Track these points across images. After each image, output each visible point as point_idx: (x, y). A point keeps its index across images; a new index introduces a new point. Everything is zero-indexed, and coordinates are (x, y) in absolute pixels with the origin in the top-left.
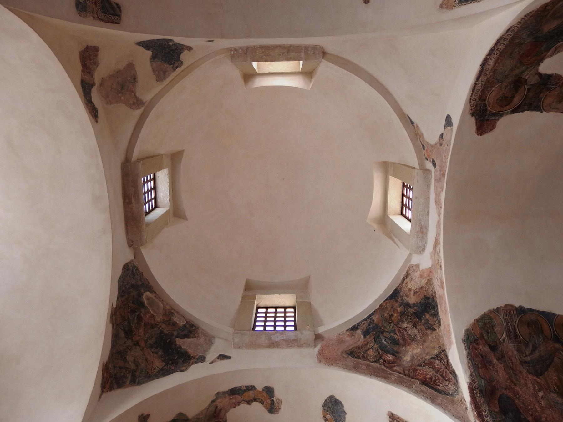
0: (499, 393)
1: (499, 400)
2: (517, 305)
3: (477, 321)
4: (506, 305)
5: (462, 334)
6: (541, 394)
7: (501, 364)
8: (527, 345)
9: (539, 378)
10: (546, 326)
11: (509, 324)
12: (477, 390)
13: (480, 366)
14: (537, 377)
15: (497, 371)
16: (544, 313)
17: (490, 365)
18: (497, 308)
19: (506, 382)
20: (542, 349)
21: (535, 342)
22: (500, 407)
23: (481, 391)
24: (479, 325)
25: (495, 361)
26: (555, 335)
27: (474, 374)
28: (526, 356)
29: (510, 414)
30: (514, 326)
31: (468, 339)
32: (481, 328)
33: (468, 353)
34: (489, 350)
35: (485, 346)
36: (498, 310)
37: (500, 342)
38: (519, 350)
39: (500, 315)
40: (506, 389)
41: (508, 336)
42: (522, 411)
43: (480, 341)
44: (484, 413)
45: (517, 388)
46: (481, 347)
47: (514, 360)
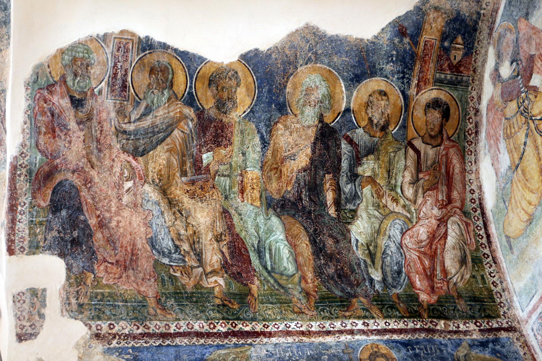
0: (59, 178)
1: (54, 189)
2: (142, 35)
3: (62, 52)
4: (122, 32)
5: (27, 73)
6: (129, 184)
7: (82, 130)
9: (136, 160)
11: (119, 65)
12: (24, 171)
13: (43, 130)
14: (134, 158)
15: (70, 142)
16: (184, 56)
17: (61, 131)
18: (105, 35)
19: (80, 161)
20: (161, 113)
21: (152, 102)
22: (51, 200)
23: (30, 172)
24: (63, 59)
25: (73, 125)
26: (190, 94)
27: (28, 143)
28: (130, 122)
29: (64, 213)
30: (126, 71)
31: (35, 82)
32: (65, 66)
33: (29, 106)
34: (69, 105)
35: (62, 97)
36: (105, 37)
37: (93, 94)
38: (121, 112)
39: (108, 47)
40: (74, 172)
41: (111, 85)
42: (85, 209)
43: (58, 89)
44: (20, 208)
45: (93, 173)
46: (55, 99)
47: (106, 126)
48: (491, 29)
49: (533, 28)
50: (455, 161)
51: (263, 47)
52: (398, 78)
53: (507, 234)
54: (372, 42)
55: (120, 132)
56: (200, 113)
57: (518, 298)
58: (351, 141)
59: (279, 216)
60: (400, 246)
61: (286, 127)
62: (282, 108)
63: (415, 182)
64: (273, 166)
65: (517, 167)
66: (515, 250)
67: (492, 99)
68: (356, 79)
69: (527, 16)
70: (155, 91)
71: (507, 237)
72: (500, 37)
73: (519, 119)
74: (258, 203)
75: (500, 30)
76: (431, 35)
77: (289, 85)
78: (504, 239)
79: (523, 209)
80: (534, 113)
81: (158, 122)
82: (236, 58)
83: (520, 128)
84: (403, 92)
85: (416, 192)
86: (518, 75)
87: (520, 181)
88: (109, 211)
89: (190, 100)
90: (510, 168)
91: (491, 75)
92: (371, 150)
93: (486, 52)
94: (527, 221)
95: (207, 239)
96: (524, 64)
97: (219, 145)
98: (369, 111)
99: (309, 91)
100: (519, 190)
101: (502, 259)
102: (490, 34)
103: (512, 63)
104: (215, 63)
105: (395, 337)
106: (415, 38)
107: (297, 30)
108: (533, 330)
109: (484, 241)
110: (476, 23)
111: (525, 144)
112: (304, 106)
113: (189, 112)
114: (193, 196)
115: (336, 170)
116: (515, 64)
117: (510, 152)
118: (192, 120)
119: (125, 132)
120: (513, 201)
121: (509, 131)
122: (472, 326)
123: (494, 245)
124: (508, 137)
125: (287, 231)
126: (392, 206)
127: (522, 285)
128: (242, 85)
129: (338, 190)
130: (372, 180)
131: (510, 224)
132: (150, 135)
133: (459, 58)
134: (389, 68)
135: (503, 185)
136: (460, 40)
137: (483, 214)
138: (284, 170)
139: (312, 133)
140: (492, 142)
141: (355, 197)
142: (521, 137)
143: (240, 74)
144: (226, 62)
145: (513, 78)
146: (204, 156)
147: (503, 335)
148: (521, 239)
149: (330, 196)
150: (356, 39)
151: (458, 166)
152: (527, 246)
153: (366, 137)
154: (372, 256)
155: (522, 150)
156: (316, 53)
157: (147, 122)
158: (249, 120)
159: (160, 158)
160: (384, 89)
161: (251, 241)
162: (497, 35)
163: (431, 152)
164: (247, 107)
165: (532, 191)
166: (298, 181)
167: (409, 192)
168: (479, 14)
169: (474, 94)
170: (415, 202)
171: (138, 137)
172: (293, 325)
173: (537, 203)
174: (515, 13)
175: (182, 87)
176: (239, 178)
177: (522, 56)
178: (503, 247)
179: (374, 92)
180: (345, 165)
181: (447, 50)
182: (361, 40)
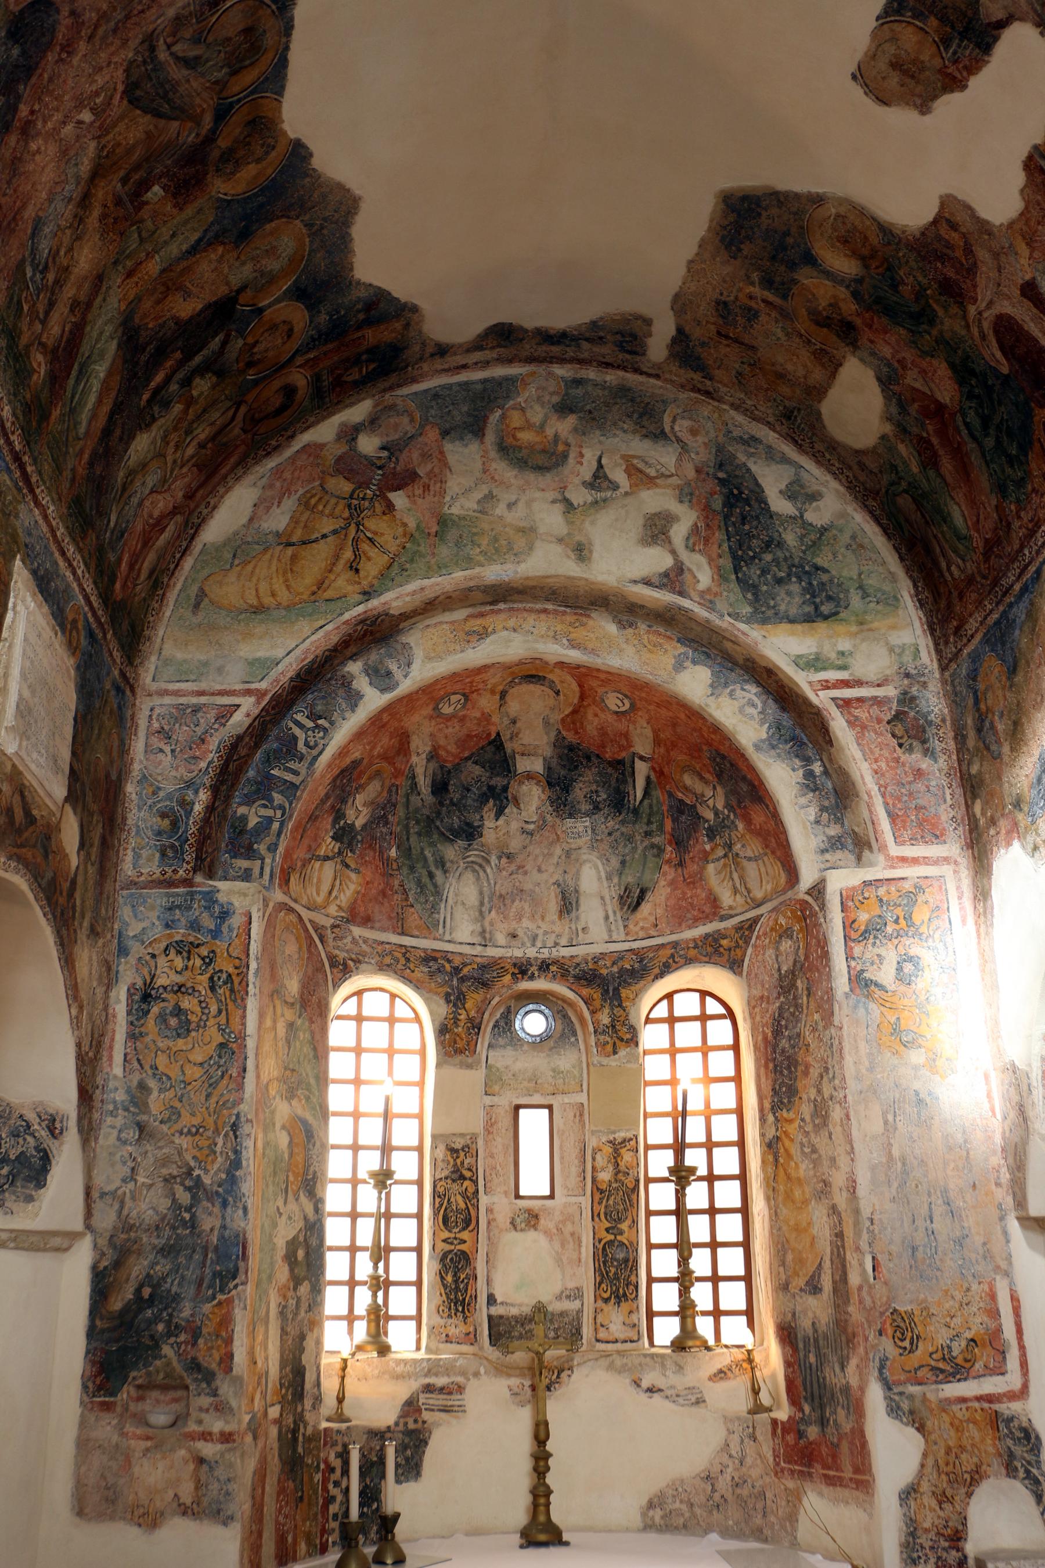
6: (86, 116)
8: (197, 40)
9: (122, 98)
10: (249, 77)
14: (123, 92)
21: (207, 60)
26: (231, 105)
48: (391, 388)
49: (442, 453)
50: (232, 460)
51: (316, 163)
52: (312, 337)
53: (207, 589)
54: (351, 283)
55: (150, 42)
56: (210, 139)
57: (160, 663)
58: (224, 343)
59: (119, 346)
60: (140, 504)
61: (222, 256)
62: (244, 235)
63: (202, 446)
64: (170, 282)
65: (290, 544)
66: (201, 614)
67: (322, 446)
68: (300, 294)
69: (445, 433)
70: (222, 55)
71: (202, 594)
72: (392, 407)
73: (340, 507)
74: (123, 307)
75: (399, 401)
76: (371, 336)
77: (273, 224)
78: (194, 590)
79: (257, 590)
80: (368, 523)
81: (181, 89)
82: (292, 135)
83: (331, 515)
84: (297, 351)
85: (192, 457)
86: (380, 468)
87: (279, 560)
88: (45, 122)
89: (222, 114)
90: (278, 534)
91: (343, 425)
92: (220, 374)
93: (364, 399)
94: (252, 606)
95: (69, 292)
96: (398, 468)
97: (175, 195)
98: (266, 335)
99: (271, 252)
100: (269, 568)
101: (171, 603)
102: (385, 391)
103: (383, 448)
104: (280, 112)
105: (89, 615)
106: (369, 322)
107: (348, 190)
108: (152, 710)
109: (172, 566)
110: (395, 371)
111: (324, 536)
112: (253, 259)
113: (208, 120)
114: (104, 217)
115: (188, 357)
116: (385, 454)
117: (294, 520)
118: (198, 135)
119: (152, 49)
120: (249, 568)
121: (313, 501)
122: (118, 661)
123: (173, 580)
124: (305, 503)
125: (110, 373)
126: (171, 450)
127: (179, 655)
128: (260, 166)
129: (168, 380)
130: (190, 402)
131: (221, 583)
132: (161, 91)
133: (349, 379)
134: (323, 318)
135: (250, 539)
136: (372, 366)
137: (193, 538)
138: (170, 298)
139: (223, 290)
140: (278, 484)
141: (166, 405)
142: (327, 525)
143: (274, 154)
144: (286, 126)
145: (371, 463)
146: (156, 188)
147: (128, 692)
148: (224, 613)
149: (159, 378)
150: (352, 264)
151: (228, 467)
152: (226, 628)
153: (234, 355)
154: (124, 488)
155: (313, 537)
156: (322, 228)
157: (177, 73)
158: (218, 208)
159: (134, 130)
160: (296, 330)
161: (85, 349)
162: (391, 402)
163: (237, 431)
164: (232, 192)
165: (288, 587)
166: (162, 326)
167: (190, 451)
168: (407, 366)
169: (312, 419)
170: (181, 467)
171: (153, 75)
172: (52, 508)
173: (285, 604)
174: (433, 412)
175: (236, 89)
176: (143, 255)
177: (404, 457)
178: (182, 595)
179: (290, 323)
180: (198, 359)
181: (357, 361)
182: (352, 270)
